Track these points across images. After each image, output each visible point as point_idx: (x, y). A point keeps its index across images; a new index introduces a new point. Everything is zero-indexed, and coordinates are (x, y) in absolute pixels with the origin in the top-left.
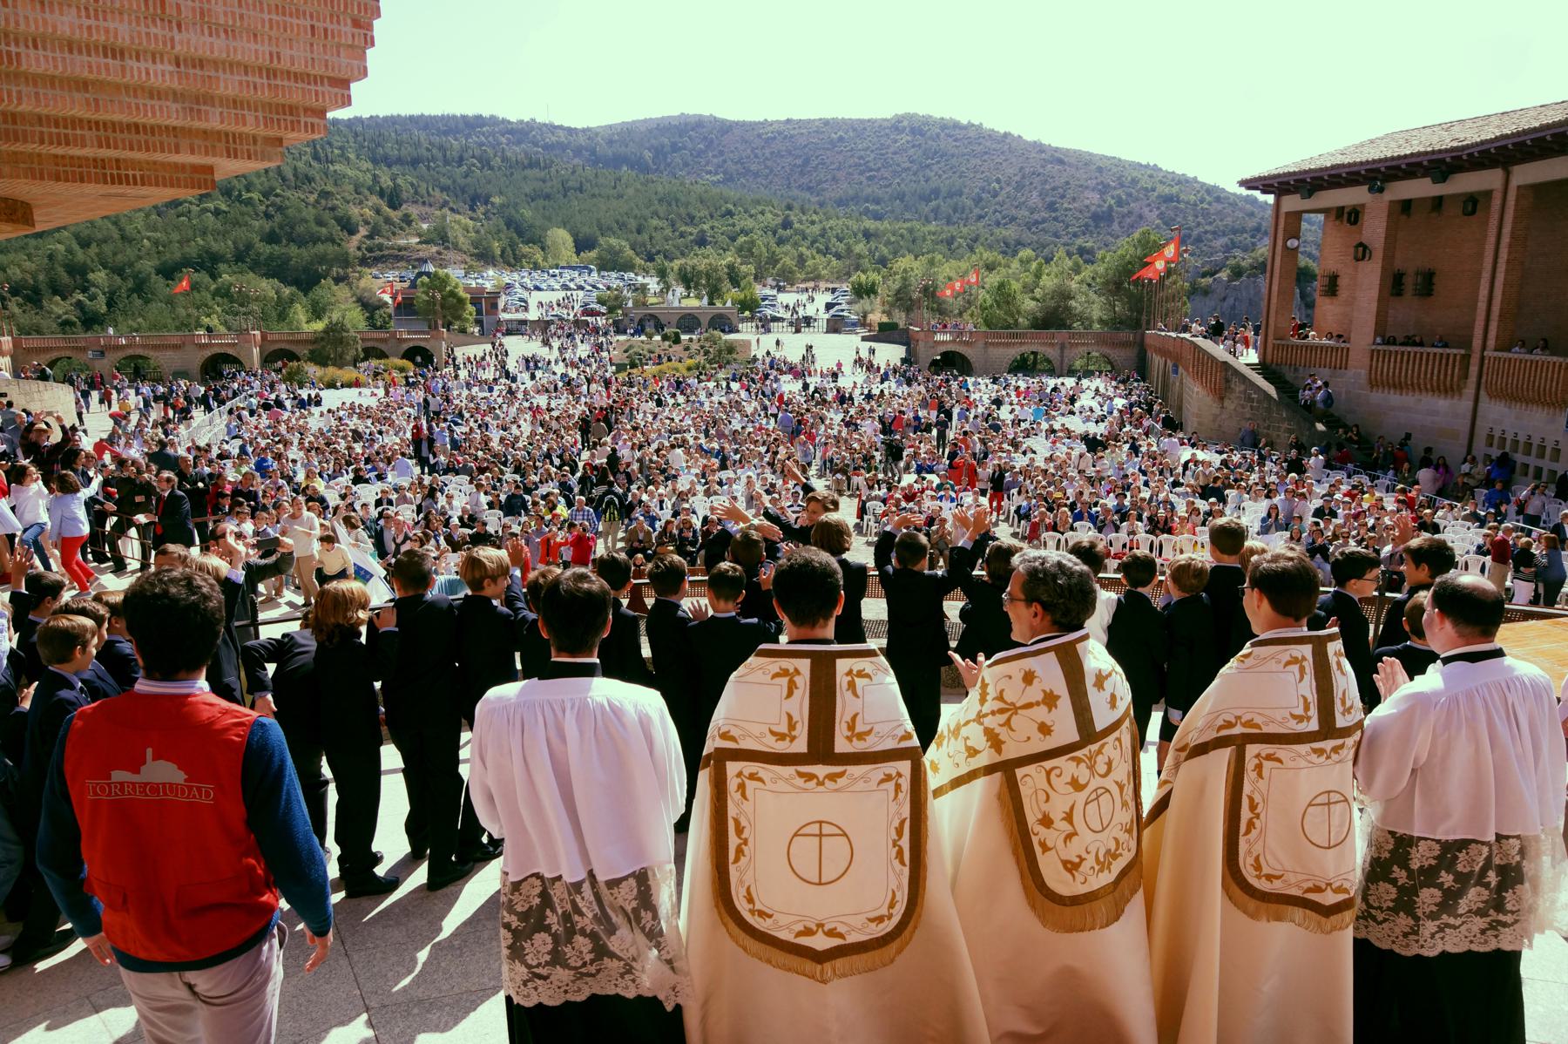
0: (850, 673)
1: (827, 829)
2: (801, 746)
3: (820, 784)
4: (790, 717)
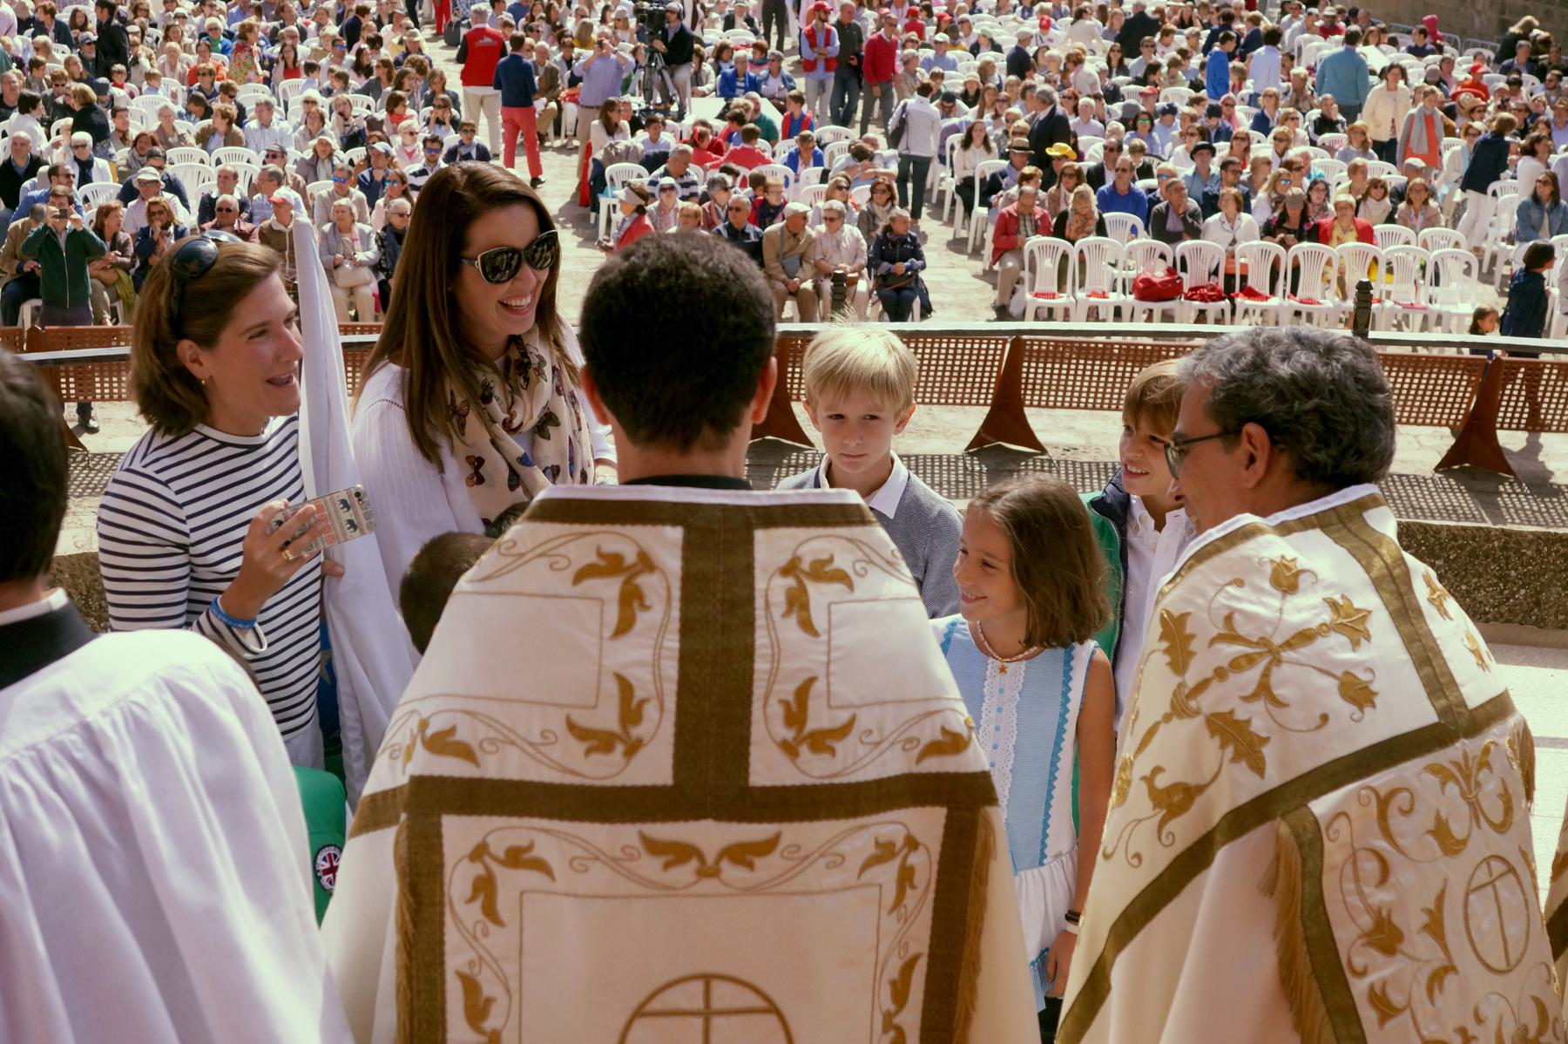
0: (790, 569)
1: (724, 995)
2: (654, 766)
3: (708, 872)
4: (625, 687)
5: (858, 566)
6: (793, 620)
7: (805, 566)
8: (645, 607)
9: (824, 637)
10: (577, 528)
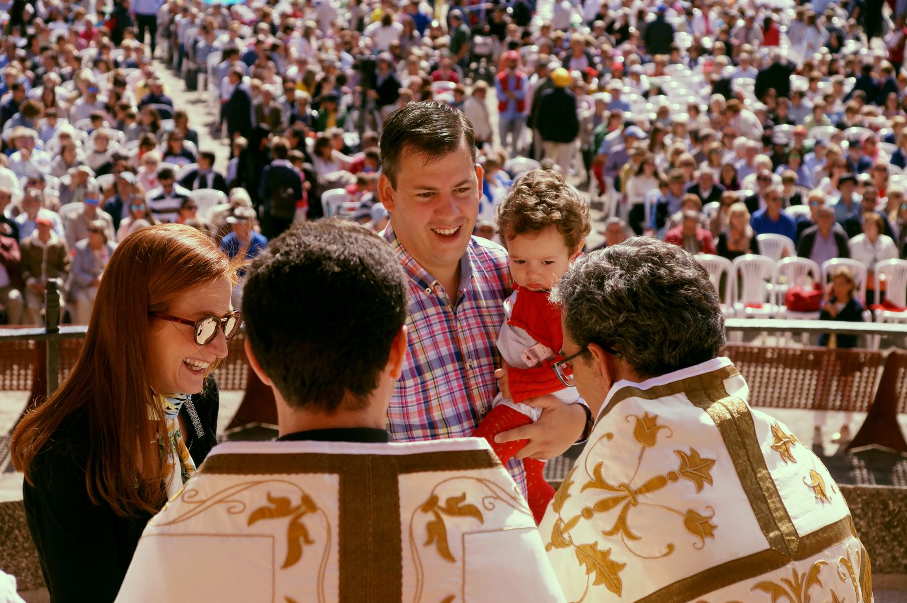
0: (431, 504)
5: (487, 502)
6: (432, 549)
7: (442, 503)
8: (308, 542)
9: (459, 563)
10: (251, 478)
